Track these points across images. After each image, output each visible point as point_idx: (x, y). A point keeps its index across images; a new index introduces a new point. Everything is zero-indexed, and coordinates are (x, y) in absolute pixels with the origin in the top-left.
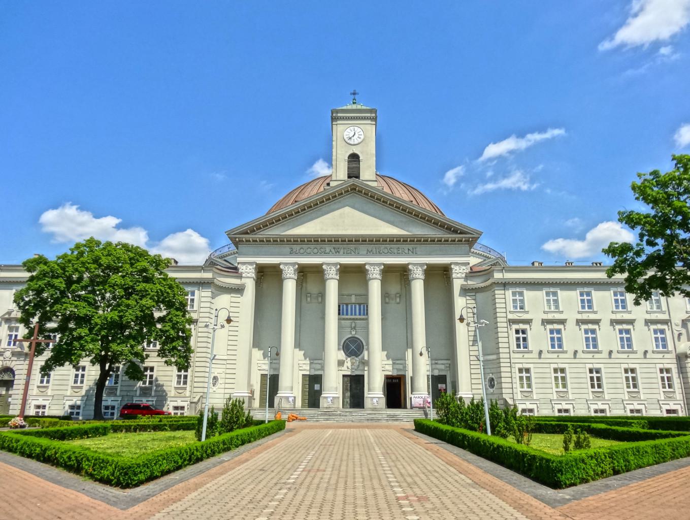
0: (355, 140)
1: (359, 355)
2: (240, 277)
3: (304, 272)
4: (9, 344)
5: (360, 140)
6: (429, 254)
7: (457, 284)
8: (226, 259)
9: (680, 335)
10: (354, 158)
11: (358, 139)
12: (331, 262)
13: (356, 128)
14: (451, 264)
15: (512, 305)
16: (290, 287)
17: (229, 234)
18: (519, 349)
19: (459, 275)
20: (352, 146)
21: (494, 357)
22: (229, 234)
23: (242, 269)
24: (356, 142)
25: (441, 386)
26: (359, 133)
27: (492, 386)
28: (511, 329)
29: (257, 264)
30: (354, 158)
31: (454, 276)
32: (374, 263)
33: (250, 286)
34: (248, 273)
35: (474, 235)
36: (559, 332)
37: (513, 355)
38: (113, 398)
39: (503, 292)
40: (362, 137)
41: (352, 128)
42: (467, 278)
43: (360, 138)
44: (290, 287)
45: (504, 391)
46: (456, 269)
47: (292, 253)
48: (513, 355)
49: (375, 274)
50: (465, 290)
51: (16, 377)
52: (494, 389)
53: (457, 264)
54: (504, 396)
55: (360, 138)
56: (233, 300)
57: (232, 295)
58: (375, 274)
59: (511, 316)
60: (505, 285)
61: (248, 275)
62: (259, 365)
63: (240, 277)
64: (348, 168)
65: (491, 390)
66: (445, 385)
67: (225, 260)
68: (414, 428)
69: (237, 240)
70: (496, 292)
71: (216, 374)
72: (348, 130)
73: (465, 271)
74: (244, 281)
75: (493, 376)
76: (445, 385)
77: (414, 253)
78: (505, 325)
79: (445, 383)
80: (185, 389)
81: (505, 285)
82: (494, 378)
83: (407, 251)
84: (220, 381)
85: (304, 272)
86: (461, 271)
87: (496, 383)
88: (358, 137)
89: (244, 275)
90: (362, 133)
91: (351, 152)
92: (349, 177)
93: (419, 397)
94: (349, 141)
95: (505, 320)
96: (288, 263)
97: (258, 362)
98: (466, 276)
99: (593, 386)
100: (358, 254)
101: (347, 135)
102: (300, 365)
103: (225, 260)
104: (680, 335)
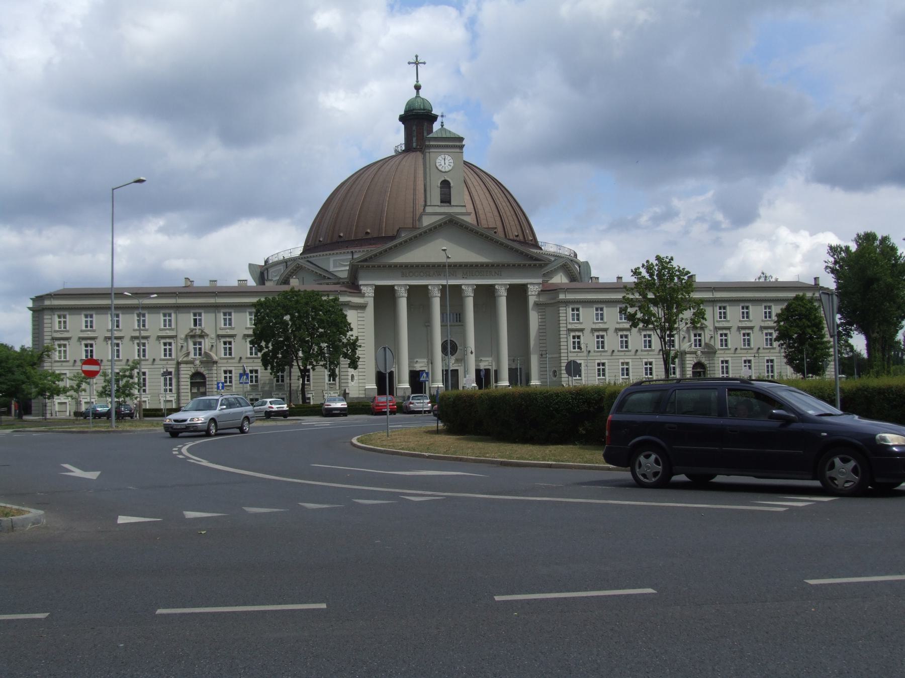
0: (446, 168)
2: (362, 295)
3: (413, 291)
4: (195, 354)
5: (450, 168)
6: (511, 277)
7: (532, 300)
8: (309, 259)
9: (684, 337)
10: (446, 184)
11: (449, 167)
12: (434, 283)
13: (447, 156)
14: (527, 284)
15: (571, 317)
16: (403, 304)
18: (575, 350)
19: (533, 293)
20: (443, 174)
21: (557, 355)
23: (364, 289)
24: (447, 169)
26: (450, 161)
27: (555, 376)
28: (569, 335)
29: (376, 286)
30: (446, 184)
31: (530, 293)
32: (468, 284)
33: (371, 302)
34: (369, 292)
36: (602, 337)
37: (570, 354)
38: (283, 393)
39: (565, 308)
40: (452, 164)
41: (443, 156)
42: (539, 295)
43: (450, 166)
44: (403, 304)
45: (563, 379)
46: (531, 288)
47: (404, 276)
48: (570, 354)
49: (469, 293)
50: (537, 304)
51: (207, 379)
53: (532, 284)
54: (563, 383)
55: (450, 166)
56: (360, 315)
57: (359, 311)
58: (469, 293)
59: (570, 327)
60: (567, 303)
61: (370, 295)
63: (362, 295)
64: (441, 194)
65: (555, 379)
67: (308, 261)
70: (561, 308)
71: (353, 373)
72: (440, 158)
73: (538, 290)
74: (366, 299)
77: (499, 275)
78: (565, 332)
80: (335, 384)
81: (567, 303)
83: (493, 273)
84: (356, 378)
85: (413, 291)
86: (535, 290)
88: (449, 165)
89: (366, 295)
90: (452, 161)
91: (443, 179)
92: (441, 202)
94: (440, 168)
95: (565, 329)
96: (401, 284)
98: (538, 294)
99: (599, 375)
100: (453, 275)
101: (438, 163)
103: (308, 261)
104: (684, 337)
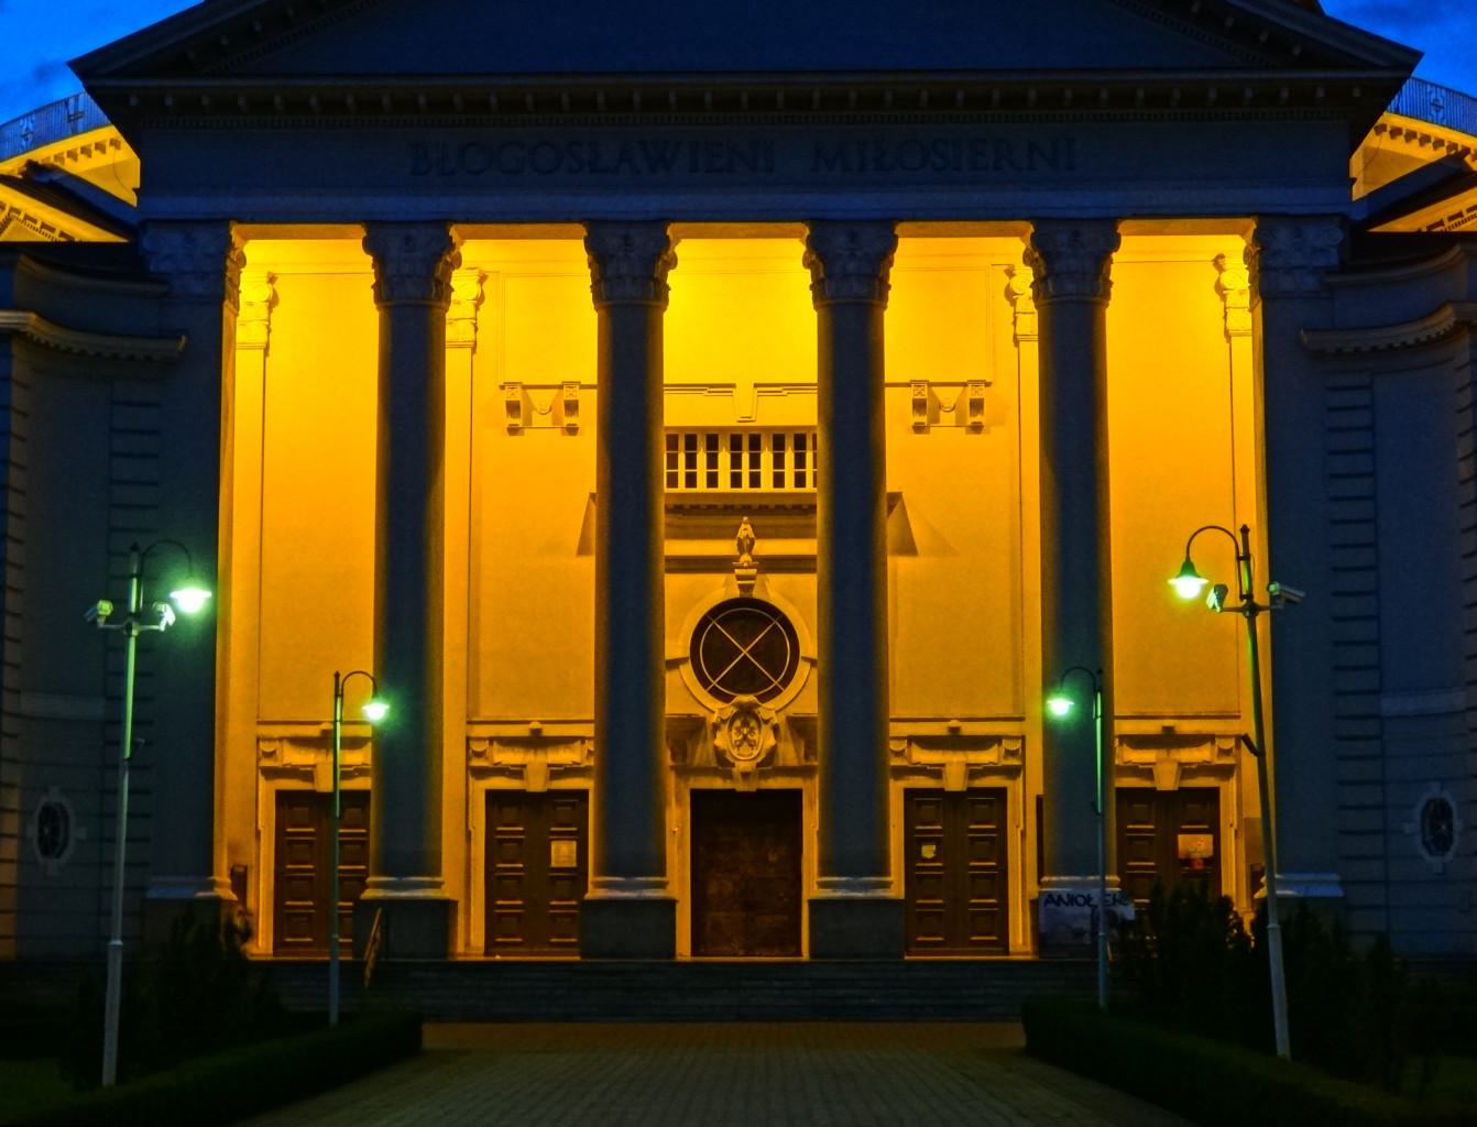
1: (776, 692)
17: (85, 68)
22: (85, 68)
25: (1195, 845)
35: (1374, 67)
52: (1449, 856)
62: (266, 747)
66: (1209, 838)
68: (1022, 1042)
69: (133, 101)
75: (1447, 796)
76: (1209, 838)
79: (1215, 830)
82: (1453, 805)
87: (1457, 824)
93: (1072, 900)
97: (264, 731)
102: (477, 747)
